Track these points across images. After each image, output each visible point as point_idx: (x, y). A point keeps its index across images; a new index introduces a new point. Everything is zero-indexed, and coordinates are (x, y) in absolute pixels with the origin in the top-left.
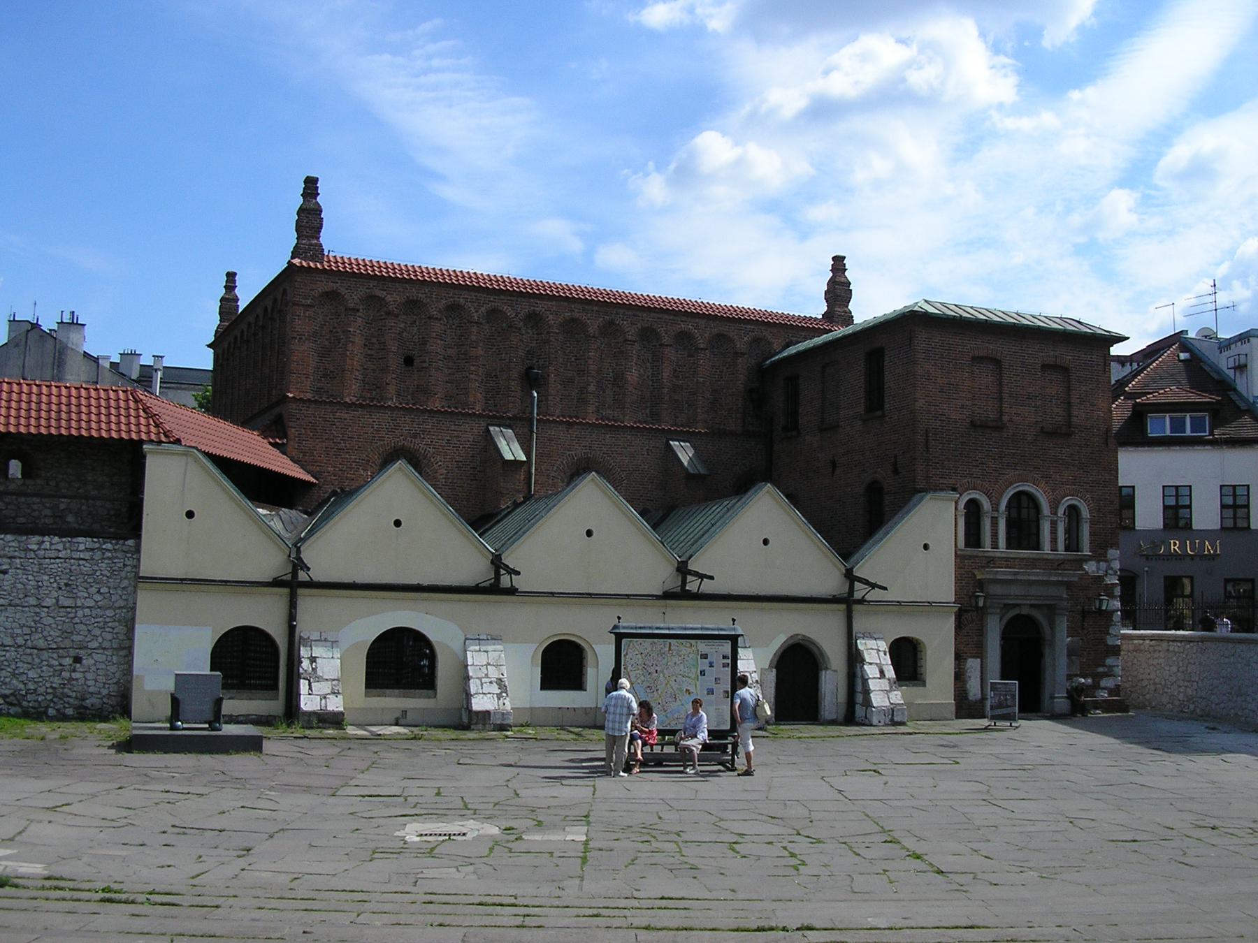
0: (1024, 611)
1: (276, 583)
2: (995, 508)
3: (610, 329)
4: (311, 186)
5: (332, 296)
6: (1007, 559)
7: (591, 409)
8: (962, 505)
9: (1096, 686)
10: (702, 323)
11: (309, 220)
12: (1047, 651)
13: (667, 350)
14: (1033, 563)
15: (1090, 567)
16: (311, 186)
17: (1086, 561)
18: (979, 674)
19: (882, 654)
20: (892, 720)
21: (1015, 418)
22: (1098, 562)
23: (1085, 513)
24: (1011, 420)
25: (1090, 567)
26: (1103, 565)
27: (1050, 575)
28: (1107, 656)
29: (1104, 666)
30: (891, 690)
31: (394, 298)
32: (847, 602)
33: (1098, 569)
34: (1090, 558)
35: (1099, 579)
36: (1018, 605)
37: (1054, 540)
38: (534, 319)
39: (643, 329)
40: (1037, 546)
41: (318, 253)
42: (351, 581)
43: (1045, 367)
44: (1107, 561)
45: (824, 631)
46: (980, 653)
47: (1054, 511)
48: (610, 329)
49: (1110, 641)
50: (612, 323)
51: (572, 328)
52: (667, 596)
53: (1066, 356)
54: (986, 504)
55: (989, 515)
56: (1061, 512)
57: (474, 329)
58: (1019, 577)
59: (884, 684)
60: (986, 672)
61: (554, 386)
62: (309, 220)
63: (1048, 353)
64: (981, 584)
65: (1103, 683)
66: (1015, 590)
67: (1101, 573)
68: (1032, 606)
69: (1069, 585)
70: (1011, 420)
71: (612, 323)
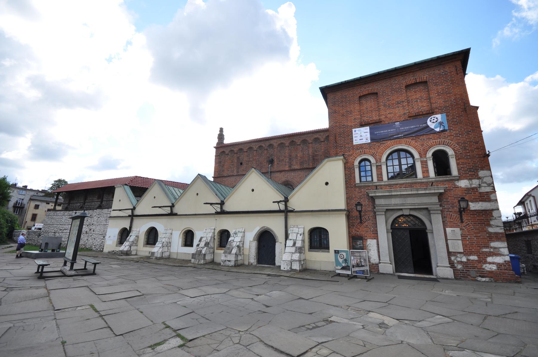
0: (407, 213)
1: (129, 216)
2: (378, 160)
3: (292, 143)
4: (221, 130)
5: (223, 152)
6: (390, 185)
7: (287, 166)
8: (356, 163)
9: (482, 260)
10: (322, 134)
11: (221, 137)
12: (430, 236)
13: (310, 145)
14: (411, 185)
15: (463, 183)
16: (221, 130)
17: (458, 180)
18: (376, 248)
19: (299, 235)
20: (291, 268)
21: (389, 116)
22: (470, 179)
23: (450, 152)
24: (386, 117)
25: (463, 183)
26: (475, 183)
27: (417, 190)
28: (494, 241)
29: (487, 247)
30: (296, 252)
31: (236, 149)
32: (287, 212)
33: (471, 185)
34: (460, 178)
35: (473, 190)
36: (401, 209)
37: (425, 171)
38: (271, 146)
39: (303, 140)
40: (416, 177)
41: (222, 143)
42: (143, 214)
43: (407, 87)
44: (479, 178)
45: (275, 225)
46: (375, 236)
47: (423, 154)
48: (292, 143)
49: (491, 230)
50: (293, 141)
51: (282, 145)
52: (217, 213)
53: (423, 76)
54: (373, 160)
55: (375, 165)
56: (430, 154)
57: (255, 152)
58: (393, 194)
59: (293, 250)
60: (379, 249)
61: (276, 163)
62: (221, 137)
63: (410, 79)
64: (373, 199)
65: (489, 259)
66: (394, 201)
67: (473, 186)
68: (411, 209)
69: (440, 195)
70: (386, 117)
71: (293, 141)
